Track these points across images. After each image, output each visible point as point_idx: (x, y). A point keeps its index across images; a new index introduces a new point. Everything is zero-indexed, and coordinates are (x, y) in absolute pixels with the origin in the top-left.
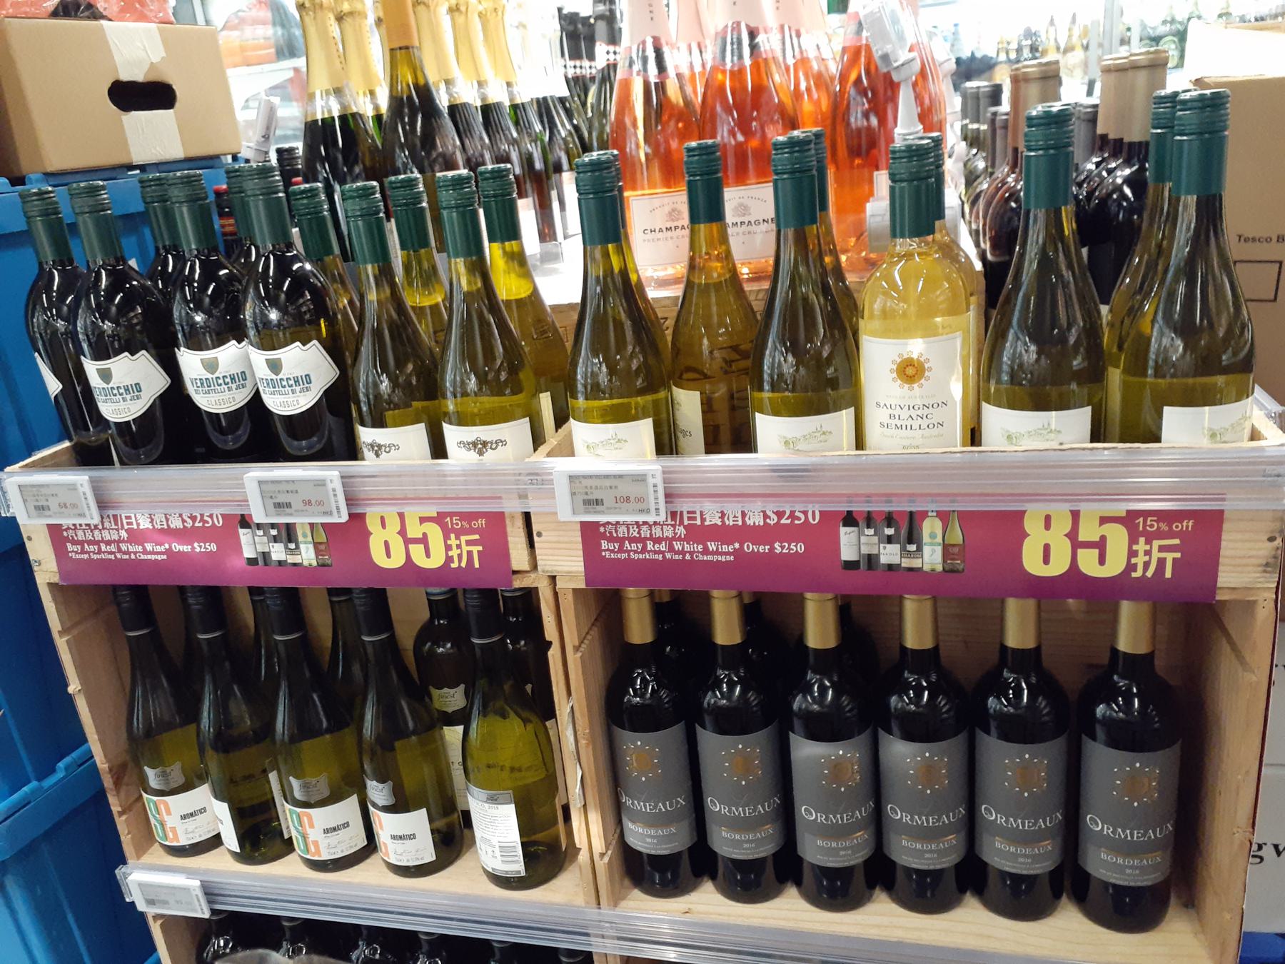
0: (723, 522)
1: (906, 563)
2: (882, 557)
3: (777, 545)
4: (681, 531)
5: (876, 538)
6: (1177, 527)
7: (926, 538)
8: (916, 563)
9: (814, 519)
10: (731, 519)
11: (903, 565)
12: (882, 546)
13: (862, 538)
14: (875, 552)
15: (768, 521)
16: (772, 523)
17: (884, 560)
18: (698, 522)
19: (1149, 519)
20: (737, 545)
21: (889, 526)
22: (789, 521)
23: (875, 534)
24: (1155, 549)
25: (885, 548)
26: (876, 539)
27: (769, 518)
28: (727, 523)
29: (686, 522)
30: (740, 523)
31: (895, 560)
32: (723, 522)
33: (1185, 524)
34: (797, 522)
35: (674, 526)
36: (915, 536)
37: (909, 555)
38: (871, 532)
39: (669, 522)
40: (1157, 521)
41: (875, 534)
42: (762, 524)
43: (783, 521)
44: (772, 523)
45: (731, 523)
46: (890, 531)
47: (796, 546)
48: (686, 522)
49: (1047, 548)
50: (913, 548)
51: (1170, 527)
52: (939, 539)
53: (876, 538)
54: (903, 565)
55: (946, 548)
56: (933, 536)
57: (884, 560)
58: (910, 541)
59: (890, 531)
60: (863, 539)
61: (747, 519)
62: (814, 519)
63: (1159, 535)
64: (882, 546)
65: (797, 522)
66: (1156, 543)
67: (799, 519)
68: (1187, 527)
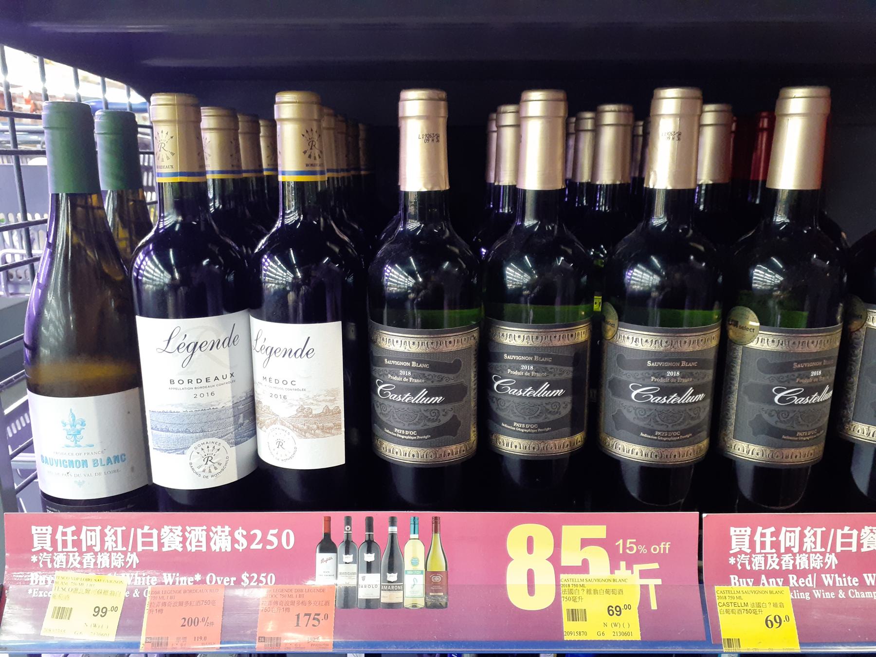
0: (184, 547)
1: (387, 598)
2: (360, 590)
3: (244, 576)
5: (356, 565)
7: (408, 566)
8: (395, 597)
9: (288, 544)
10: (194, 544)
11: (383, 601)
12: (361, 575)
13: (340, 566)
14: (352, 582)
15: (236, 546)
16: (241, 548)
17: (362, 594)
18: (155, 548)
20: (198, 577)
21: (369, 551)
22: (260, 547)
23: (354, 562)
25: (364, 579)
26: (354, 567)
27: (238, 542)
28: (189, 548)
30: (204, 549)
31: (374, 594)
32: (184, 547)
34: (269, 547)
36: (396, 562)
37: (388, 586)
38: (349, 558)
40: (636, 544)
41: (354, 562)
42: (229, 549)
43: (254, 546)
44: (241, 548)
45: (194, 549)
46: (370, 558)
47: (266, 577)
49: (530, 550)
50: (393, 577)
51: (649, 550)
52: (421, 566)
53: (356, 565)
54: (383, 601)
55: (429, 575)
56: (415, 562)
57: (362, 594)
58: (391, 569)
59: (370, 558)
60: (342, 568)
61: (212, 544)
62: (288, 544)
64: (361, 575)
65: (269, 547)
67: (271, 543)
68: (665, 548)
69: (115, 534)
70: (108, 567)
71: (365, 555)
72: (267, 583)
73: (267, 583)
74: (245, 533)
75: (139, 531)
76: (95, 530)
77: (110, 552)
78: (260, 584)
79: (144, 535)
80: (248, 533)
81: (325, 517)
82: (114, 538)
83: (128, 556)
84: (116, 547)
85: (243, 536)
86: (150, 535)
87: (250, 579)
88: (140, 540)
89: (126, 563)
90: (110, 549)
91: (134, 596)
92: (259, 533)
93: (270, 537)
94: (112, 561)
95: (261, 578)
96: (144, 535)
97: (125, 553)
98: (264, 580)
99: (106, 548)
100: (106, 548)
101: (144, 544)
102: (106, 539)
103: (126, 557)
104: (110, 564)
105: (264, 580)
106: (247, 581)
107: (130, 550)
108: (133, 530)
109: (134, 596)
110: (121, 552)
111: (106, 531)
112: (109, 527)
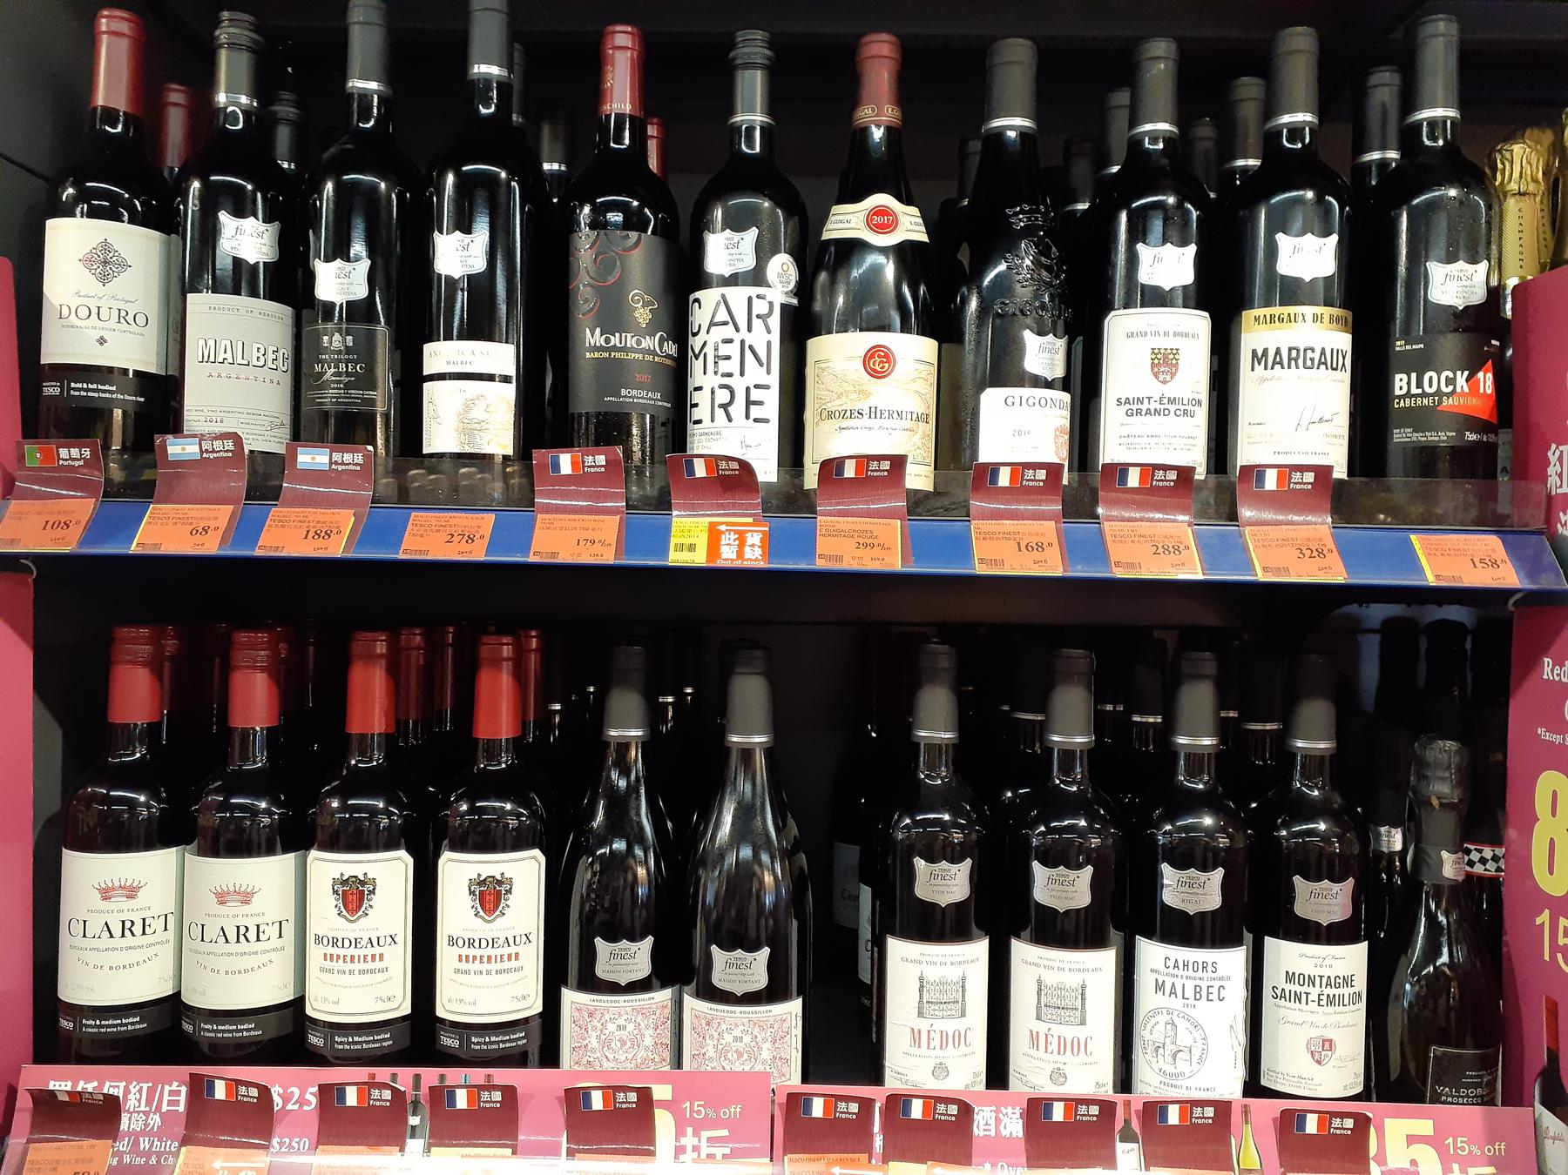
4: (156, 1120)
6: (725, 1113)
19: (697, 1103)
24: (704, 1144)
29: (165, 1108)
33: (732, 1110)
34: (306, 1108)
35: (146, 1114)
39: (143, 1108)
43: (289, 1107)
47: (298, 1143)
48: (165, 1108)
63: (708, 1124)
65: (306, 1108)
66: (705, 1134)
67: (309, 1103)
69: (140, 1091)
70: (126, 1130)
71: (410, 1117)
72: (299, 1149)
73: (299, 1149)
74: (281, 1092)
75: (167, 1088)
76: (118, 1087)
77: (131, 1113)
78: (291, 1151)
79: (171, 1093)
80: (285, 1091)
81: (369, 1074)
82: (138, 1097)
83: (150, 1118)
84: (139, 1106)
85: (279, 1095)
86: (178, 1093)
87: (281, 1144)
88: (166, 1098)
89: (146, 1125)
90: (131, 1110)
91: (151, 1163)
92: (296, 1091)
93: (308, 1097)
94: (132, 1124)
95: (294, 1144)
96: (171, 1093)
97: (146, 1114)
98: (296, 1145)
99: (127, 1108)
100: (127, 1108)
101: (170, 1103)
102: (129, 1097)
103: (147, 1118)
104: (129, 1128)
105: (296, 1145)
106: (277, 1146)
107: (153, 1110)
108: (160, 1086)
109: (151, 1163)
110: (144, 1113)
111: (131, 1087)
112: (135, 1083)
